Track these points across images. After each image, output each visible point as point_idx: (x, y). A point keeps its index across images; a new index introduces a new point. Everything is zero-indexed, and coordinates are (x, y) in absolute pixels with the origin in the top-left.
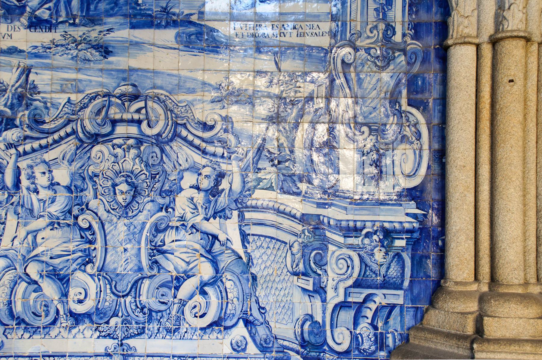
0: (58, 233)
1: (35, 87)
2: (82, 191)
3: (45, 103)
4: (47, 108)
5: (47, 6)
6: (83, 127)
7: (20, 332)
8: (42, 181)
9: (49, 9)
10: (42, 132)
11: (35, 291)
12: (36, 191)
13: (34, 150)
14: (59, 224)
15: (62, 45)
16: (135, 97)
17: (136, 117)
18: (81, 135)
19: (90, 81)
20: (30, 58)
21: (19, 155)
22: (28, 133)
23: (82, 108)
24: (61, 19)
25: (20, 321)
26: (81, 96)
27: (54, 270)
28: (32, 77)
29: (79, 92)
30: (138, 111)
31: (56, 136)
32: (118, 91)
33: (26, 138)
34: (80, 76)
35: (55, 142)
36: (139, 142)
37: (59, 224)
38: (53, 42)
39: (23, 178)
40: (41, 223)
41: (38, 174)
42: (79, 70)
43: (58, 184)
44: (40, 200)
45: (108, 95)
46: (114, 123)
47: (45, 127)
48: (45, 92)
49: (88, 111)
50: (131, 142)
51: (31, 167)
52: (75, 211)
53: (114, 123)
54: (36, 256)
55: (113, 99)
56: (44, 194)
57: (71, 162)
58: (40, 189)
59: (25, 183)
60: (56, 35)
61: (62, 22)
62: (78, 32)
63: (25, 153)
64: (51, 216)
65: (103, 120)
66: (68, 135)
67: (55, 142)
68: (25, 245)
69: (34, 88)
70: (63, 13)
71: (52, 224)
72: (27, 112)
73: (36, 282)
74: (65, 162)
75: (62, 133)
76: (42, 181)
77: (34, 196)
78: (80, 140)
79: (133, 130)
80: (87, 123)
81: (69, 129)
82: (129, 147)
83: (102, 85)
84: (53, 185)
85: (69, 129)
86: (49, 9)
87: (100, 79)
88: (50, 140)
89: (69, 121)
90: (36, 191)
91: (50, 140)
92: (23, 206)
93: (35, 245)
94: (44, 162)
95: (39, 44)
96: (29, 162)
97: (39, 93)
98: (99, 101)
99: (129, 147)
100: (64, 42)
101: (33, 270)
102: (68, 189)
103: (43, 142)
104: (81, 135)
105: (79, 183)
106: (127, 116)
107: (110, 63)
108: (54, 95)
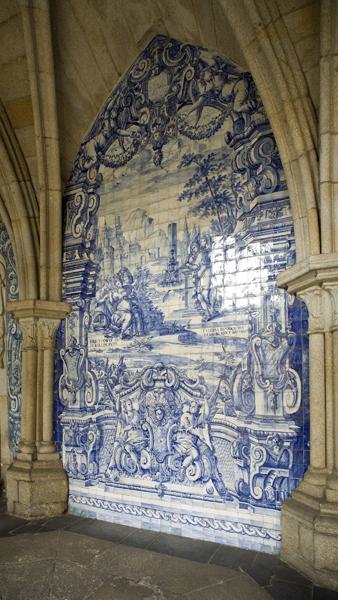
0: (135, 432)
8: (129, 408)
16: (162, 368)
36: (165, 390)
40: (129, 427)
45: (152, 368)
46: (155, 381)
53: (155, 381)
56: (130, 414)
59: (123, 409)
60: (131, 342)
62: (140, 339)
76: (129, 408)
79: (162, 384)
83: (150, 363)
101: (127, 448)
106: (160, 378)
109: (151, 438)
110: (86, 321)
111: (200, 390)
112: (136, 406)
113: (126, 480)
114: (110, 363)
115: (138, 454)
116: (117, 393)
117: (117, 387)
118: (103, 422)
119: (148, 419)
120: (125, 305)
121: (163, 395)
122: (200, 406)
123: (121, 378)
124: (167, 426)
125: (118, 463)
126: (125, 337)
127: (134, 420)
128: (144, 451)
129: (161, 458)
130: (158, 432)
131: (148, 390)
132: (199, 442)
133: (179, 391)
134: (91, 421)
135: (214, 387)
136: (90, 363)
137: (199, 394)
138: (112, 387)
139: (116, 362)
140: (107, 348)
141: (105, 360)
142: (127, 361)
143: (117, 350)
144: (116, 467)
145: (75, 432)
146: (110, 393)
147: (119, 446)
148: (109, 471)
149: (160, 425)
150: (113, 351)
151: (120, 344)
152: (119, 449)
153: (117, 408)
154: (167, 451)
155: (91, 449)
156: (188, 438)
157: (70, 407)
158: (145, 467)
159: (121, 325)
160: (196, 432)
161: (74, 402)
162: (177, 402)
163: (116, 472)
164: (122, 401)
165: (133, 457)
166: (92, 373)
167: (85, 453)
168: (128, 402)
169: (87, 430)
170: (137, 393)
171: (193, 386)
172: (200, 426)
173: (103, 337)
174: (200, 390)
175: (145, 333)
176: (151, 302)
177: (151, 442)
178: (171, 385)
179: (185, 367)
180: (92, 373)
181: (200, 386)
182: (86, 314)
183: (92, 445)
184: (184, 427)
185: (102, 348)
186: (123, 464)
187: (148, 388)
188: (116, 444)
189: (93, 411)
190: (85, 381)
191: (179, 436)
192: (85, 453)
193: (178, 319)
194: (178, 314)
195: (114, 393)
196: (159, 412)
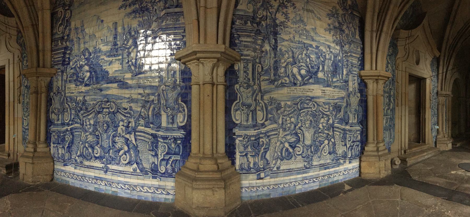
0: (91, 136)
1: (86, 100)
6: (96, 110)
8: (88, 123)
12: (87, 126)
13: (86, 116)
16: (108, 102)
17: (108, 107)
21: (83, 117)
22: (85, 112)
26: (96, 102)
28: (85, 98)
30: (109, 105)
31: (90, 112)
32: (104, 100)
33: (85, 113)
34: (96, 97)
36: (109, 113)
40: (88, 134)
42: (95, 96)
45: (102, 101)
46: (103, 108)
47: (88, 110)
49: (97, 105)
50: (107, 113)
52: (95, 131)
53: (103, 108)
56: (88, 126)
57: (94, 118)
59: (85, 124)
60: (90, 88)
62: (95, 86)
64: (90, 132)
66: (93, 112)
69: (86, 101)
70: (92, 82)
71: (90, 134)
73: (87, 148)
75: (92, 111)
76: (88, 123)
79: (107, 110)
80: (97, 109)
81: (93, 110)
82: (107, 115)
83: (100, 99)
84: (90, 124)
85: (93, 110)
89: (93, 108)
90: (87, 126)
91: (89, 113)
93: (87, 139)
99: (107, 115)
101: (87, 145)
102: (93, 125)
103: (88, 114)
105: (95, 124)
106: (106, 107)
109: (100, 140)
110: (65, 78)
111: (130, 113)
112: (92, 122)
114: (78, 99)
115: (93, 148)
117: (82, 112)
118: (74, 131)
119: (99, 129)
120: (87, 68)
121: (108, 116)
122: (129, 122)
123: (84, 107)
124: (110, 133)
126: (86, 85)
127: (90, 130)
128: (96, 147)
129: (106, 150)
130: (105, 136)
132: (129, 142)
133: (117, 114)
134: (67, 130)
135: (138, 112)
136: (67, 99)
137: (129, 115)
138: (79, 112)
139: (81, 98)
140: (77, 91)
141: (75, 98)
142: (87, 98)
143: (82, 92)
145: (58, 136)
146: (78, 115)
147: (82, 144)
148: (77, 158)
149: (106, 132)
151: (83, 89)
154: (110, 147)
155: (67, 146)
156: (122, 140)
157: (55, 123)
158: (97, 155)
159: (84, 79)
160: (127, 136)
161: (58, 120)
162: (116, 120)
164: (84, 119)
165: (90, 150)
166: (68, 104)
168: (87, 120)
169: (65, 135)
171: (126, 111)
172: (129, 133)
173: (74, 86)
174: (130, 113)
175: (98, 83)
177: (100, 142)
178: (113, 110)
179: (121, 101)
180: (68, 104)
181: (130, 111)
182: (65, 74)
183: (67, 143)
184: (120, 134)
185: (74, 91)
186: (84, 154)
187: (99, 112)
188: (81, 143)
189: (68, 125)
190: (64, 109)
191: (117, 139)
192: (63, 147)
193: (117, 75)
194: (117, 72)
195: (80, 115)
196: (105, 125)
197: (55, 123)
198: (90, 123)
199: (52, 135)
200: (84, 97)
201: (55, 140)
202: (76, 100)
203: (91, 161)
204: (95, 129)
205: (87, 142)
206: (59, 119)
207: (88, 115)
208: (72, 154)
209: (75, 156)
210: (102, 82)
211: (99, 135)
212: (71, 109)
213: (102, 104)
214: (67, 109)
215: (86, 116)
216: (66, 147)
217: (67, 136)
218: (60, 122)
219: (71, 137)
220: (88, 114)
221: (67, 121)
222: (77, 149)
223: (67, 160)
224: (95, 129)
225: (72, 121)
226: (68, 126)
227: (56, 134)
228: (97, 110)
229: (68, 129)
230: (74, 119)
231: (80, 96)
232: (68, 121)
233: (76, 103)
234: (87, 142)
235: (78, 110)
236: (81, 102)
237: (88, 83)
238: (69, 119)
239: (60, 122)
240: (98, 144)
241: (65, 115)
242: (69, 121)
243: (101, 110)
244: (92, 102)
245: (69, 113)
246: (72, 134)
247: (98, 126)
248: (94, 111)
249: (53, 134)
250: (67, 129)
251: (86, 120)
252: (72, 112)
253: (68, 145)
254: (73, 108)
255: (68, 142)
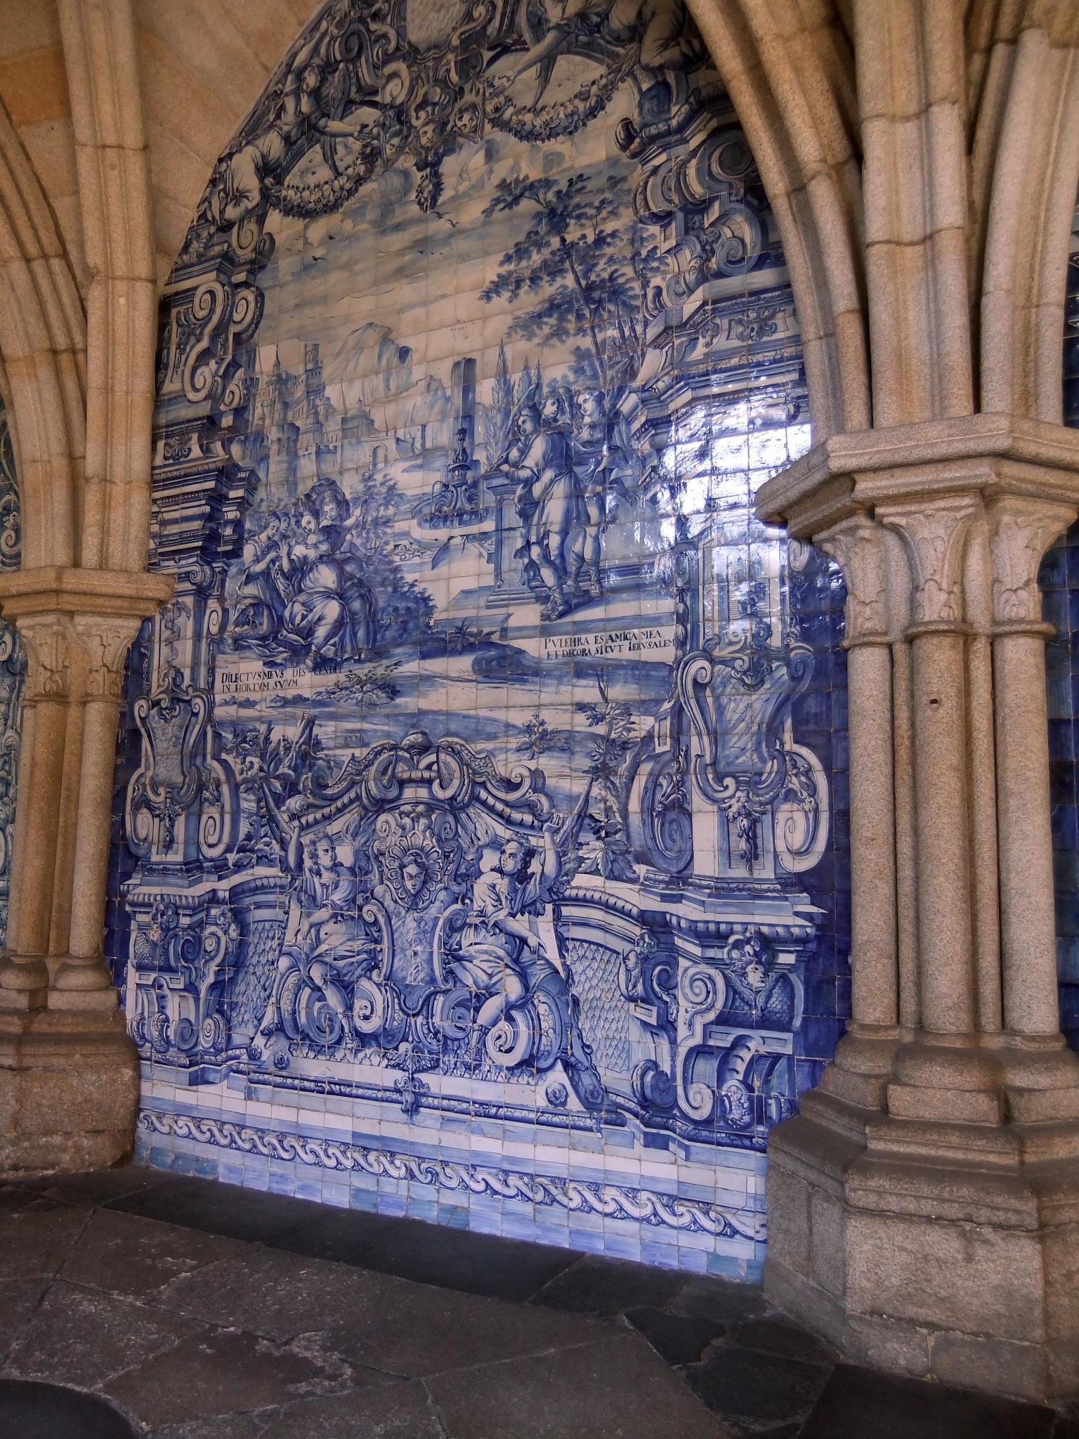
0: (341, 927)
1: (318, 743)
2: (366, 874)
3: (328, 762)
4: (330, 768)
5: (332, 642)
6: (368, 791)
7: (305, 1050)
8: (325, 860)
9: (334, 645)
10: (325, 798)
11: (319, 1000)
12: (319, 874)
13: (317, 822)
14: (342, 915)
15: (347, 688)
18: (365, 801)
19: (376, 731)
20: (315, 707)
21: (302, 828)
22: (311, 800)
23: (366, 766)
24: (346, 656)
25: (305, 1037)
26: (366, 751)
27: (338, 974)
28: (316, 730)
29: (366, 745)
31: (339, 804)
33: (310, 806)
34: (366, 726)
35: (339, 810)
37: (342, 915)
38: (337, 685)
39: (306, 856)
40: (323, 914)
41: (321, 853)
42: (363, 718)
43: (342, 865)
44: (323, 885)
45: (394, 748)
47: (329, 792)
48: (329, 749)
49: (373, 769)
51: (314, 843)
52: (360, 901)
54: (319, 955)
55: (400, 753)
56: (327, 877)
57: (355, 836)
58: (323, 871)
59: (308, 863)
60: (341, 676)
61: (347, 660)
62: (363, 670)
63: (309, 826)
64: (334, 906)
65: (389, 780)
66: (351, 801)
67: (339, 810)
68: (309, 941)
69: (318, 745)
70: (348, 648)
71: (334, 916)
72: (310, 774)
73: (319, 989)
74: (349, 836)
75: (346, 799)
76: (325, 860)
77: (316, 880)
78: (365, 808)
80: (372, 785)
81: (352, 794)
83: (388, 735)
84: (336, 866)
85: (352, 794)
86: (334, 645)
87: (386, 728)
88: (333, 808)
89: (353, 784)
90: (319, 874)
91: (333, 808)
92: (306, 892)
93: (319, 941)
94: (327, 836)
95: (323, 689)
96: (311, 836)
97: (323, 749)
98: (385, 756)
100: (348, 684)
101: (317, 973)
102: (352, 870)
103: (326, 811)
104: (365, 801)
105: (363, 864)
107: (397, 706)
108: (339, 752)
109: (385, 945)
112: (345, 854)
113: (313, 1067)
114: (275, 736)
115: (347, 988)
116: (293, 817)
117: (294, 803)
118: (247, 901)
119: (379, 890)
123: (306, 778)
125: (287, 1016)
126: (322, 664)
127: (338, 897)
128: (364, 983)
131: (379, 812)
134: (213, 898)
138: (279, 801)
139: (294, 732)
141: (263, 728)
142: (325, 731)
143: (299, 700)
144: (280, 1028)
145: (165, 929)
146: (272, 820)
147: (293, 967)
148: (260, 1041)
150: (286, 702)
151: (306, 682)
152: (292, 980)
153: (292, 860)
155: (211, 979)
157: (155, 858)
161: (169, 845)
163: (280, 1044)
164: (305, 840)
165: (333, 998)
166: (224, 764)
167: (191, 988)
168: (322, 846)
169: (201, 924)
170: (349, 818)
175: (378, 654)
176: (396, 570)
180: (224, 764)
183: (213, 967)
186: (303, 1019)
187: (381, 805)
188: (284, 963)
189: (220, 869)
190: (201, 787)
192: (191, 988)
195: (283, 818)
197: (155, 858)
198: (334, 858)
199: (133, 925)
200: (310, 723)
201: (146, 950)
202: (267, 739)
203: (339, 1055)
204: (362, 893)
205: (319, 959)
206: (172, 841)
207: (328, 818)
208: (235, 1022)
209: (251, 1032)
210: (399, 650)
211: (382, 921)
212: (237, 786)
213: (398, 759)
214: (218, 786)
215: (317, 822)
216: (203, 988)
217: (213, 929)
218: (176, 857)
219: (234, 932)
220: (326, 811)
221: (214, 853)
222: (263, 995)
223: (206, 1052)
224: (362, 893)
225: (242, 849)
226: (220, 878)
227: (155, 918)
228: (374, 791)
229: (221, 894)
230: (249, 837)
231: (289, 720)
232: (222, 847)
233: (262, 757)
234: (319, 959)
235: (273, 794)
236: (293, 753)
237: (331, 655)
238: (226, 838)
239: (179, 858)
240: (376, 967)
241: (204, 818)
242: (229, 849)
243: (393, 793)
244: (349, 752)
245: (227, 807)
246: (239, 917)
247: (375, 876)
248: (358, 797)
249: (140, 918)
250: (214, 891)
251: (314, 843)
252: (244, 805)
253: (217, 973)
254: (245, 781)
255: (218, 960)
